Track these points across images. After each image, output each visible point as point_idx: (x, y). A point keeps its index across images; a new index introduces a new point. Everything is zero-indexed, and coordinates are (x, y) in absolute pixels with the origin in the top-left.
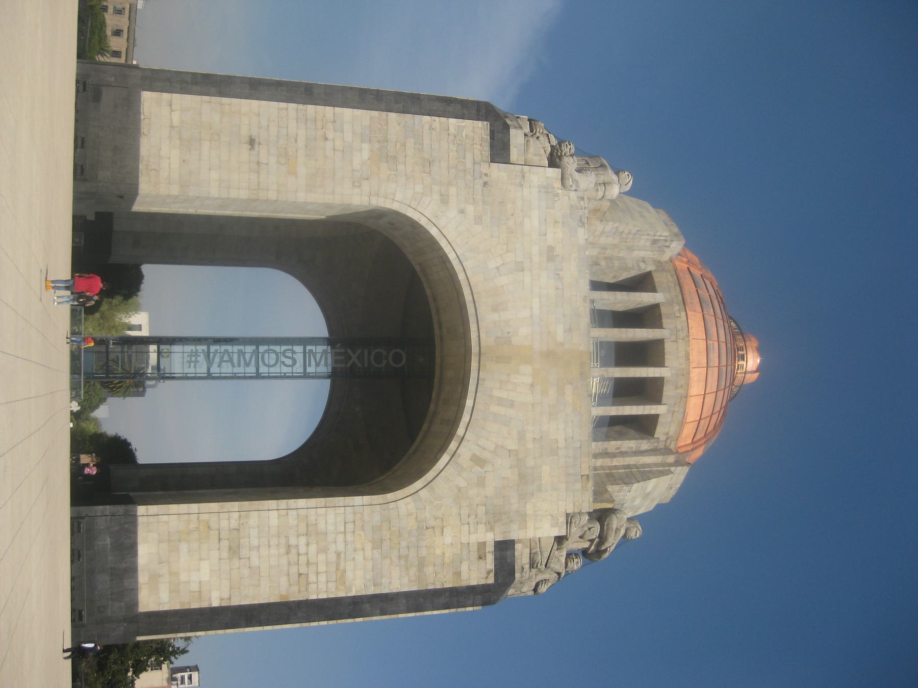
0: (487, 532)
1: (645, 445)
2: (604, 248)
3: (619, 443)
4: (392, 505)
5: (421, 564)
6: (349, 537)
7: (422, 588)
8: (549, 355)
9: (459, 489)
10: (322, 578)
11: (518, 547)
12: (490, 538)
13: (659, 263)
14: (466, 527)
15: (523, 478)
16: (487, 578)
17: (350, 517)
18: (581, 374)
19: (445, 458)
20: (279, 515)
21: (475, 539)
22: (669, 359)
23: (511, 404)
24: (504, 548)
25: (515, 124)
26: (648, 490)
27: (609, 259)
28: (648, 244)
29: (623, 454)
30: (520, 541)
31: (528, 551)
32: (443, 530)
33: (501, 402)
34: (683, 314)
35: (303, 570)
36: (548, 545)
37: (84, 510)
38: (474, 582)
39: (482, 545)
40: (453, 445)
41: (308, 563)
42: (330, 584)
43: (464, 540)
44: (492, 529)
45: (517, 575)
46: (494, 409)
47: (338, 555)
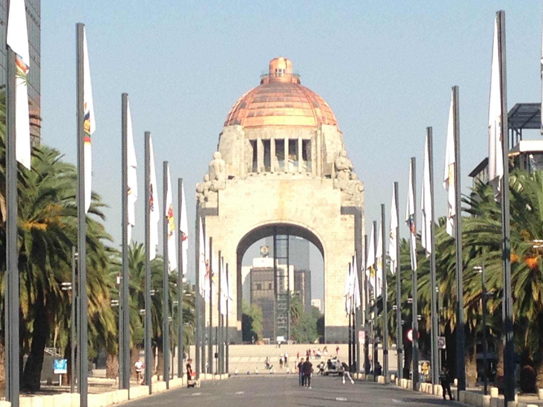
1: (313, 143)
2: (241, 160)
3: (312, 155)
4: (328, 249)
5: (346, 240)
7: (354, 239)
8: (281, 195)
9: (324, 227)
11: (344, 205)
12: (340, 216)
13: (246, 136)
15: (320, 205)
16: (352, 218)
18: (287, 183)
19: (314, 232)
22: (282, 138)
23: (297, 209)
24: (343, 211)
25: (203, 204)
26: (330, 143)
27: (245, 158)
28: (239, 141)
29: (316, 153)
30: (342, 204)
31: (346, 202)
34: (265, 129)
36: (343, 194)
37: (325, 341)
38: (353, 222)
39: (342, 219)
40: (310, 229)
45: (353, 205)
47: (342, 266)
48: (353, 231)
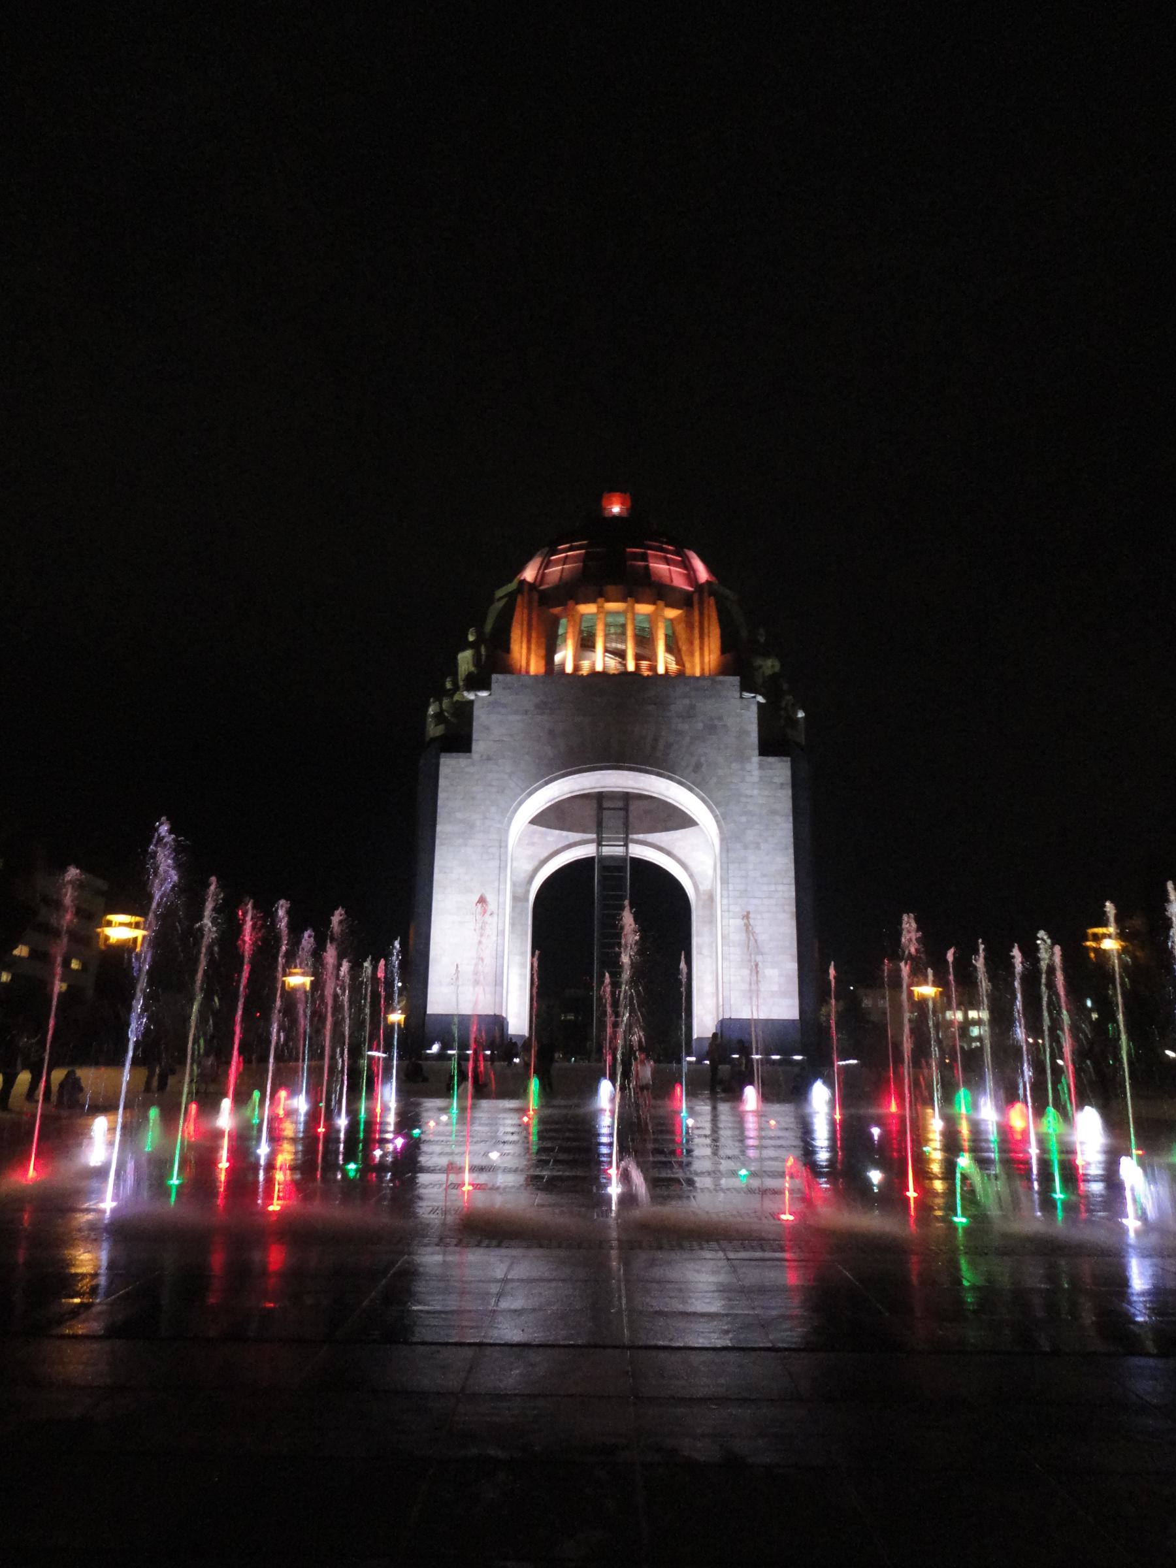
0: (750, 762)
6: (751, 866)
10: (780, 888)
12: (756, 759)
14: (748, 779)
17: (736, 865)
20: (732, 918)
21: (756, 773)
32: (751, 796)
33: (654, 748)
35: (773, 901)
38: (789, 773)
39: (761, 767)
41: (769, 897)
42: (784, 883)
43: (756, 779)
44: (748, 759)
46: (659, 754)
47: (764, 876)
48: (790, 792)
